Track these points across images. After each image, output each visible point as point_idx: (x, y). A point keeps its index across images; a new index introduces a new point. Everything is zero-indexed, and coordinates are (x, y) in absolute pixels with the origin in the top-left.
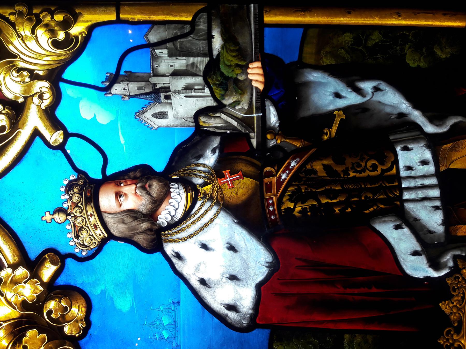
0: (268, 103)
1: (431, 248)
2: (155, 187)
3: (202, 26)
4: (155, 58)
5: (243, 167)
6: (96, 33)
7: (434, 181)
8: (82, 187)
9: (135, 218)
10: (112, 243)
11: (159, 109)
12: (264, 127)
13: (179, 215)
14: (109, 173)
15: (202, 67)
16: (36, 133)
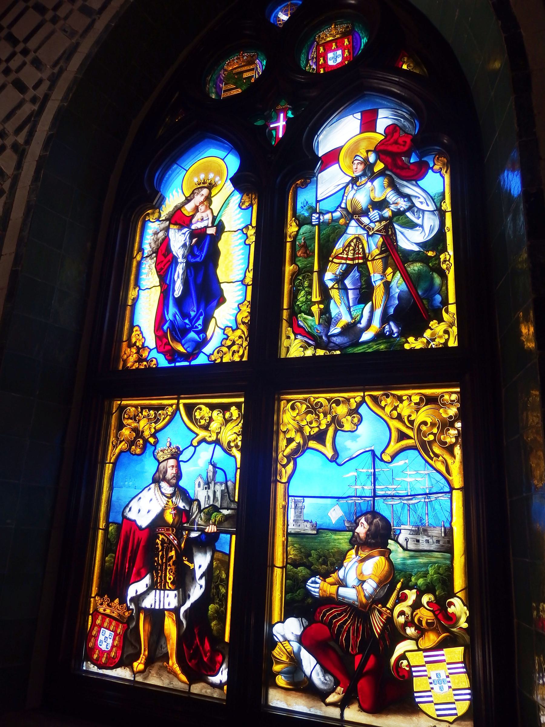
0: (200, 533)
1: (138, 599)
3: (233, 506)
7: (162, 607)
8: (177, 453)
9: (164, 473)
10: (157, 464)
11: (202, 484)
12: (191, 530)
13: (163, 490)
14: (181, 463)
15: (216, 504)
16: (197, 435)
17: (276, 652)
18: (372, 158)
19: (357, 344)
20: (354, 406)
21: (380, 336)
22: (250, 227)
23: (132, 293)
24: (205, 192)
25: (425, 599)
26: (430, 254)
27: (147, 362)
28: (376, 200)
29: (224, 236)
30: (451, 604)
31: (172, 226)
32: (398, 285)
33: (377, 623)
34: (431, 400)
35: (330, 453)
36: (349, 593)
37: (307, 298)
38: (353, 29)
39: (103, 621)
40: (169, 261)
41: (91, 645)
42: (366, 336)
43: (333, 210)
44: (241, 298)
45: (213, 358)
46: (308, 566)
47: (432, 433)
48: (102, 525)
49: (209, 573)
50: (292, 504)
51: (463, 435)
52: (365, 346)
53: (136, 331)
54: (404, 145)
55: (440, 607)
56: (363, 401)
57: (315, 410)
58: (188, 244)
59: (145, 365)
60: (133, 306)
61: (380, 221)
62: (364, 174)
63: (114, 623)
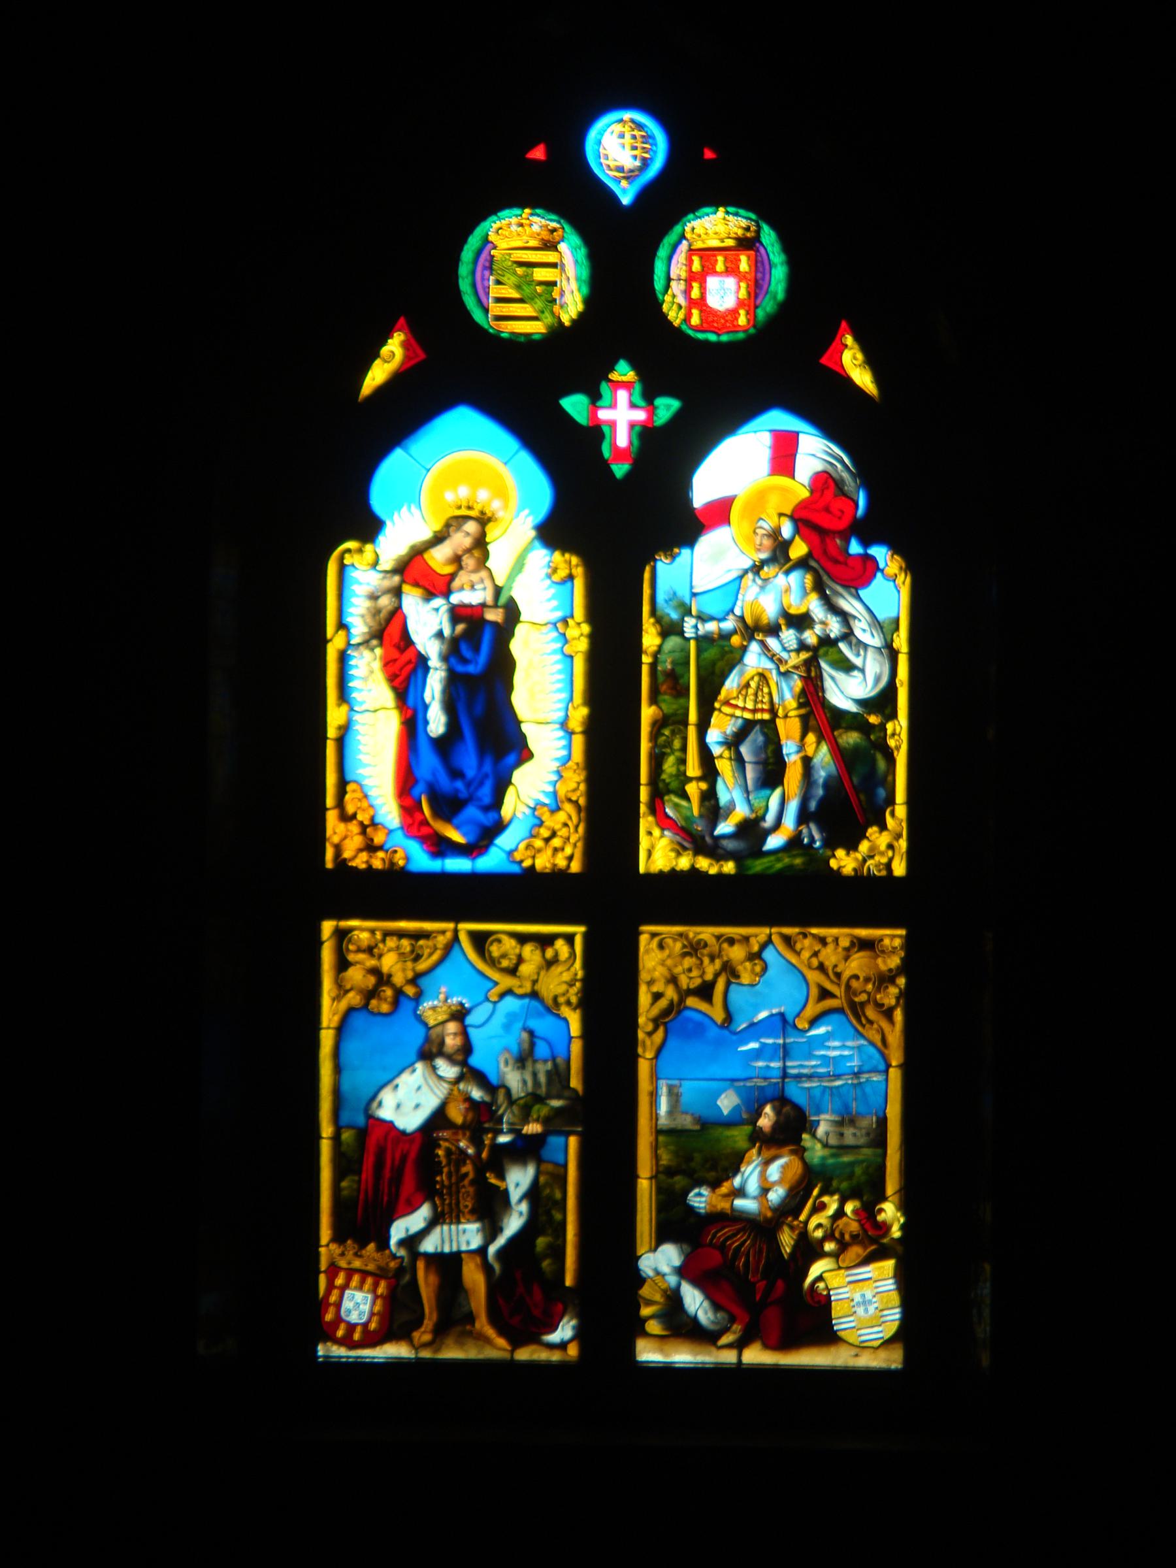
1: (411, 1242)
2: (460, 1058)
4: (545, 1061)
5: (470, 1116)
6: (563, 1024)
7: (455, 1249)
11: (511, 1062)
13: (441, 1073)
15: (539, 1092)
16: (496, 984)
17: (645, 1291)
18: (787, 530)
20: (756, 948)
21: (794, 843)
22: (570, 621)
23: (335, 716)
24: (471, 527)
26: (873, 719)
27: (387, 851)
28: (792, 611)
29: (519, 630)
30: (881, 1210)
31: (406, 588)
33: (787, 1240)
35: (718, 1015)
37: (678, 770)
38: (757, 238)
40: (410, 662)
41: (329, 1317)
42: (774, 842)
43: (720, 616)
45: (518, 856)
47: (865, 991)
48: (327, 1130)
49: (533, 1194)
50: (663, 1091)
51: (907, 997)
52: (772, 858)
53: (354, 791)
54: (840, 518)
55: (868, 1213)
56: (769, 941)
57: (696, 950)
59: (383, 860)
60: (341, 742)
61: (798, 651)
62: (772, 560)
63: (369, 1281)
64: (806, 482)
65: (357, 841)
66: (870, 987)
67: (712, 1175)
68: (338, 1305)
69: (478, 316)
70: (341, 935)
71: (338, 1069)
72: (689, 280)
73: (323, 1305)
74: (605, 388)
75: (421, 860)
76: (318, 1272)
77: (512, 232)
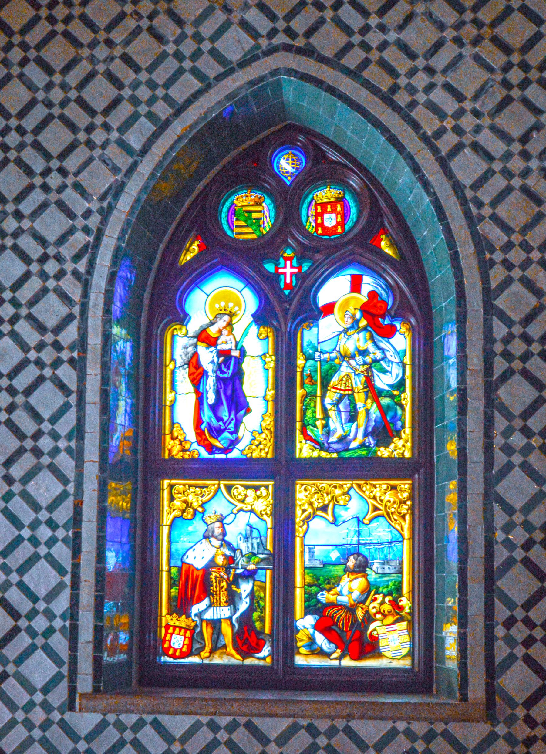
1: (199, 615)
17: (299, 636)
18: (358, 315)
19: (347, 450)
20: (346, 490)
21: (362, 445)
23: (169, 396)
25: (387, 599)
26: (396, 393)
28: (361, 348)
29: (246, 359)
31: (199, 343)
32: (375, 412)
33: (360, 613)
34: (394, 488)
35: (331, 519)
36: (344, 600)
39: (174, 630)
41: (166, 646)
42: (353, 445)
44: (265, 410)
45: (245, 452)
46: (318, 586)
48: (165, 567)
49: (252, 594)
58: (216, 361)
60: (172, 407)
61: (363, 365)
62: (352, 327)
63: (183, 631)
64: (366, 295)
65: (178, 447)
66: (395, 506)
67: (327, 586)
68: (170, 641)
69: (229, 233)
70: (171, 486)
71: (170, 542)
72: (317, 215)
73: (164, 641)
74: (282, 261)
75: (204, 454)
76: (161, 627)
77: (242, 199)
